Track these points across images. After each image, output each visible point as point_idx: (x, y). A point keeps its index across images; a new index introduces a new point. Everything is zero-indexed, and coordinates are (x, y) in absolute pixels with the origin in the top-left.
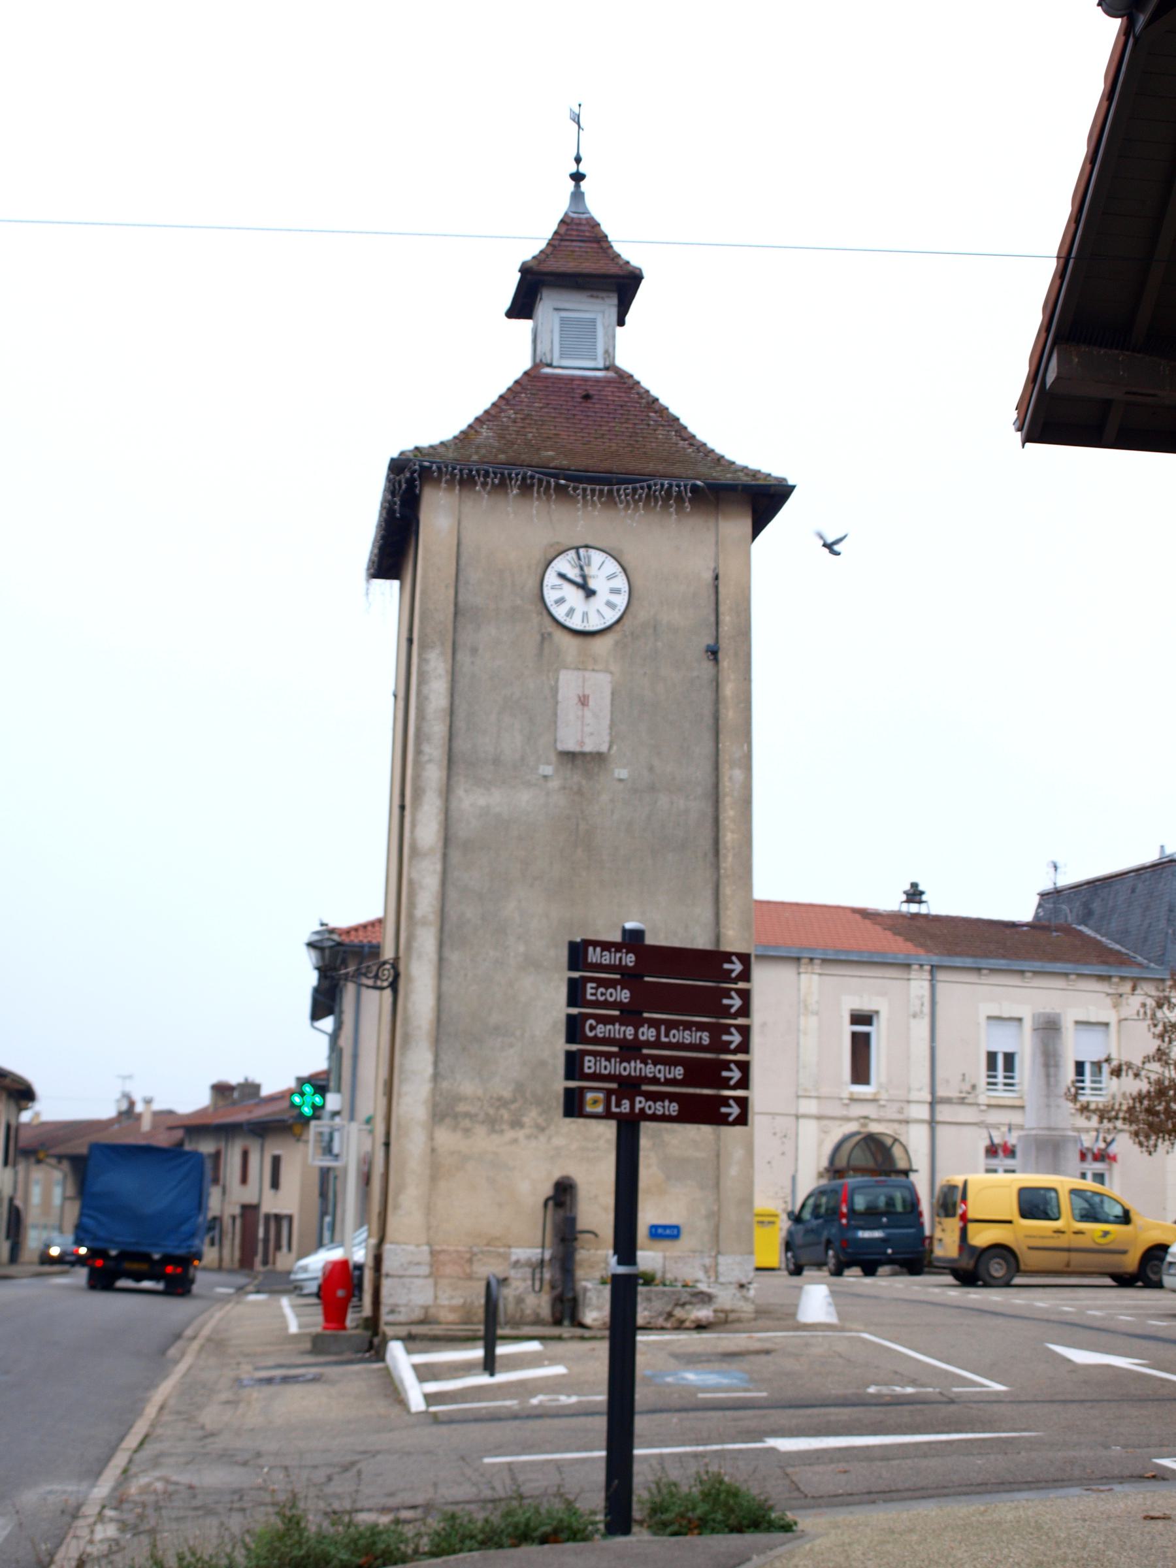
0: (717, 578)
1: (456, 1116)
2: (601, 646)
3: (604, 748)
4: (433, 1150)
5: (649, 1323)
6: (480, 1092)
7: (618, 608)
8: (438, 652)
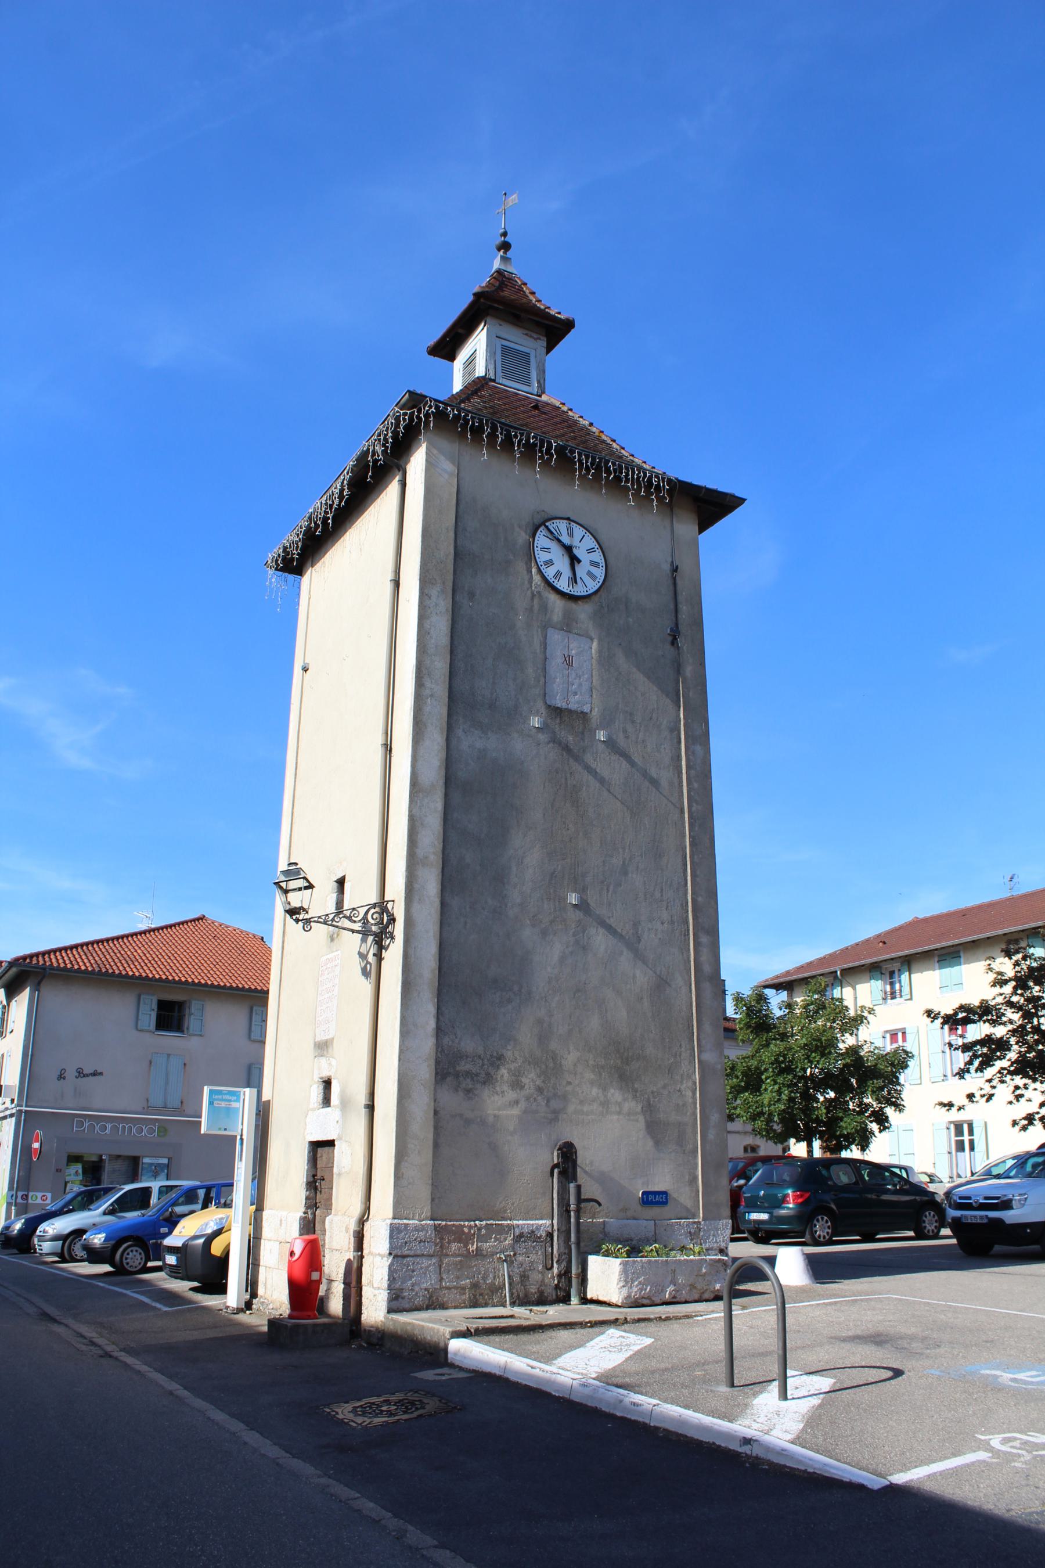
0: (675, 570)
1: (457, 1075)
2: (583, 612)
3: (586, 709)
4: (436, 1113)
5: (674, 1297)
6: (480, 1050)
7: (598, 580)
8: (439, 590)
